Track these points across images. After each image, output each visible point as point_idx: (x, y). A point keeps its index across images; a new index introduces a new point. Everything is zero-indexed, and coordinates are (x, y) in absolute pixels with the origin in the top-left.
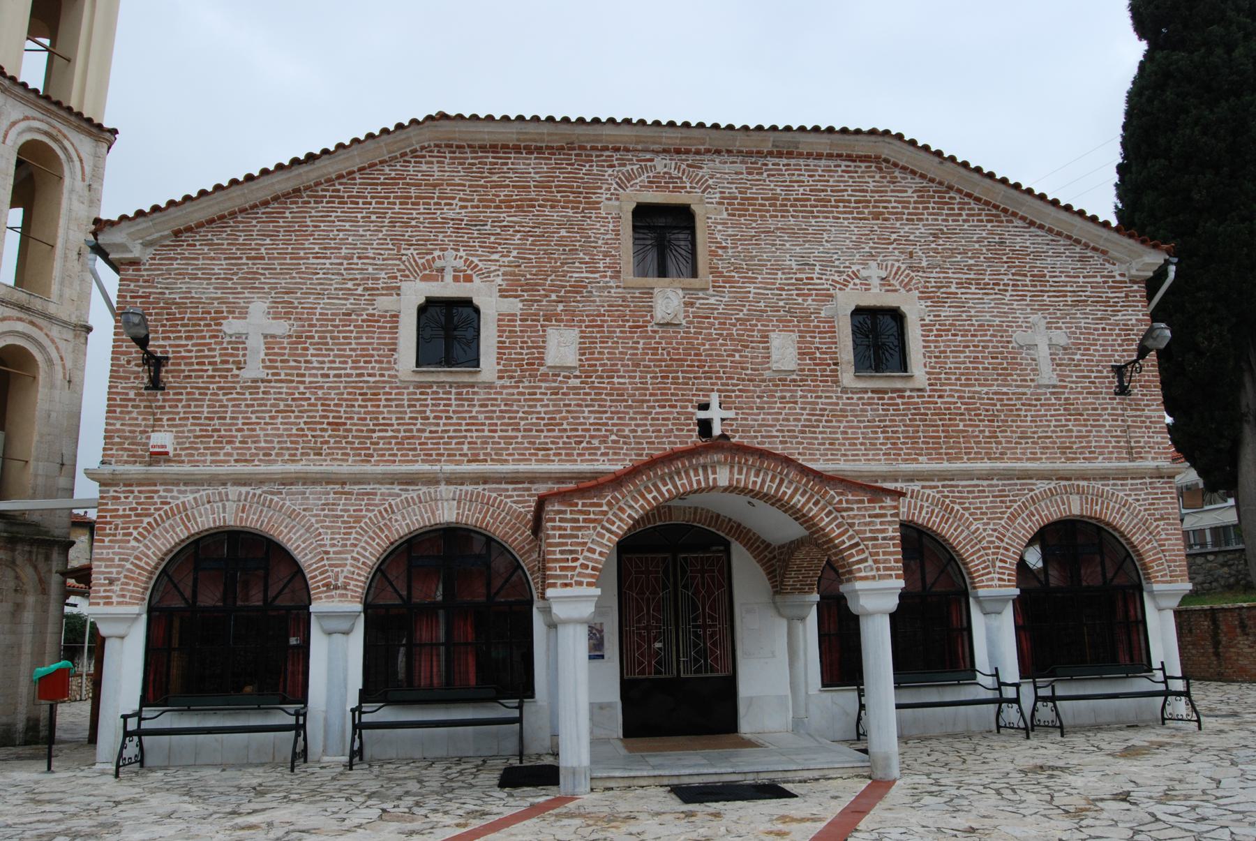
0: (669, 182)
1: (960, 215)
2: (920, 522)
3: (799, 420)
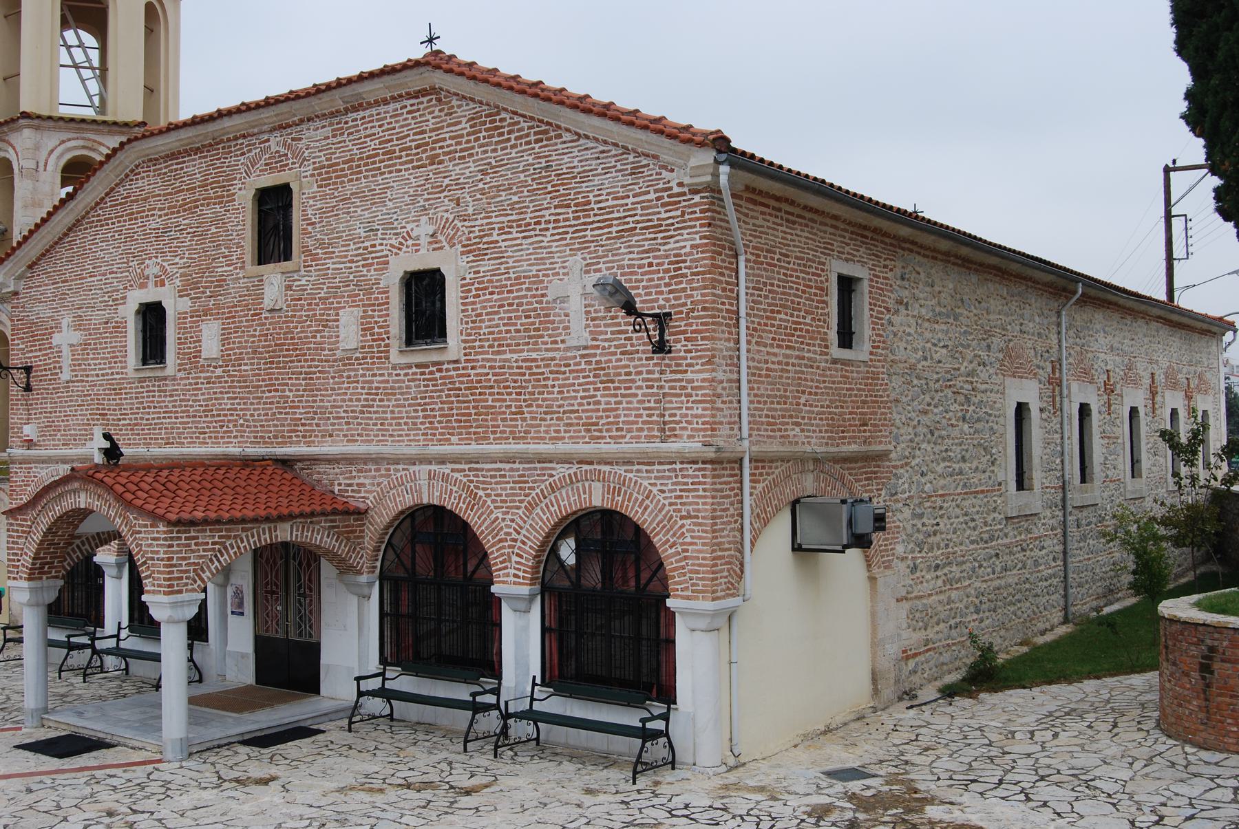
1: (509, 140)
2: (449, 507)
3: (359, 400)
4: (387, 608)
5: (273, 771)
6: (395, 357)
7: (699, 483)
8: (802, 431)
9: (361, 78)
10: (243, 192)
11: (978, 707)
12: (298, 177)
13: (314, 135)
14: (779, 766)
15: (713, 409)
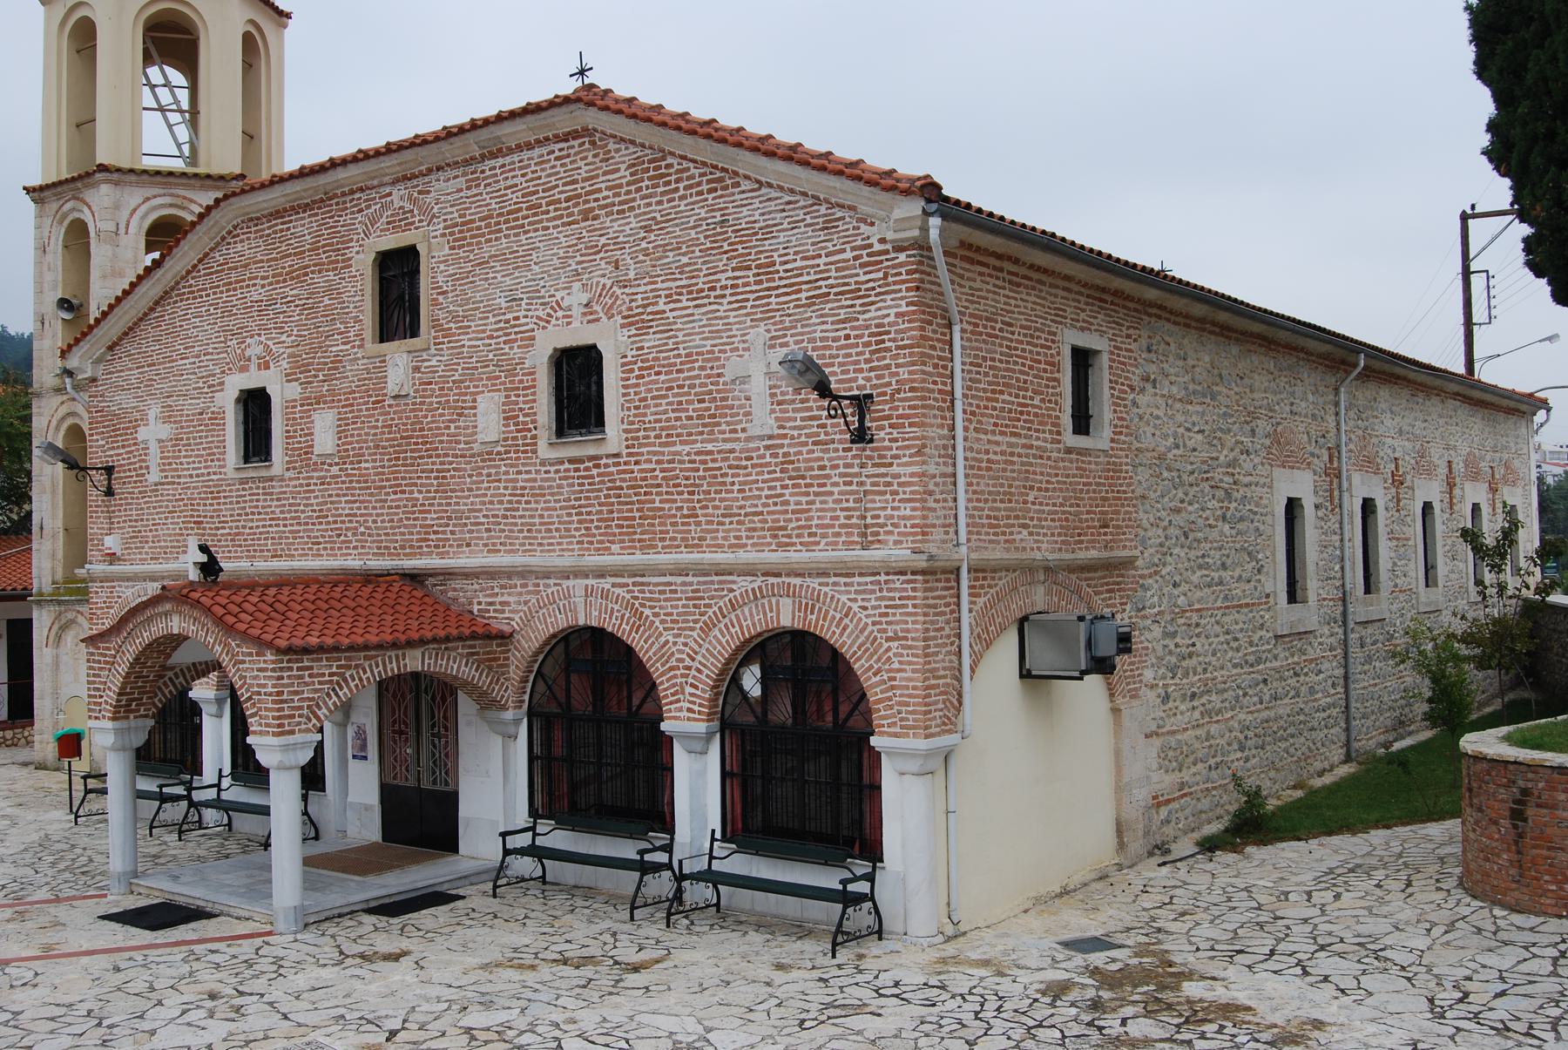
0: (401, 221)
1: (677, 189)
3: (501, 502)
4: (537, 750)
5: (405, 944)
6: (544, 451)
7: (908, 598)
8: (1031, 534)
9: (500, 118)
10: (361, 256)
11: (1244, 863)
12: (427, 238)
13: (444, 187)
14: (1006, 935)
15: (923, 509)
